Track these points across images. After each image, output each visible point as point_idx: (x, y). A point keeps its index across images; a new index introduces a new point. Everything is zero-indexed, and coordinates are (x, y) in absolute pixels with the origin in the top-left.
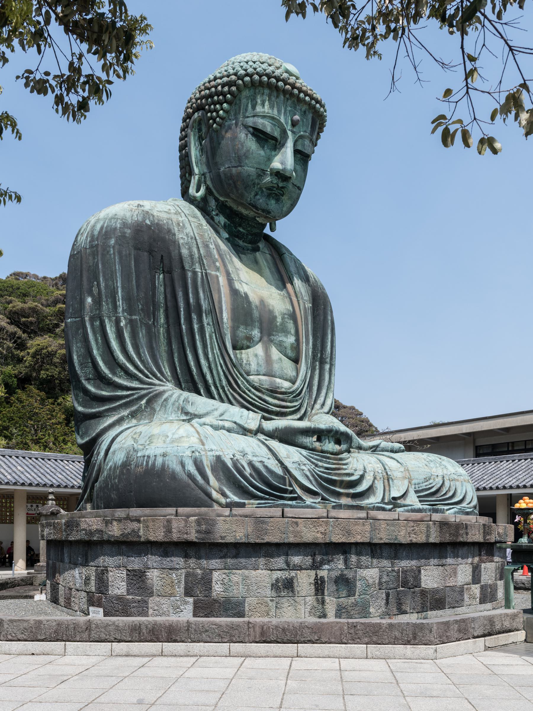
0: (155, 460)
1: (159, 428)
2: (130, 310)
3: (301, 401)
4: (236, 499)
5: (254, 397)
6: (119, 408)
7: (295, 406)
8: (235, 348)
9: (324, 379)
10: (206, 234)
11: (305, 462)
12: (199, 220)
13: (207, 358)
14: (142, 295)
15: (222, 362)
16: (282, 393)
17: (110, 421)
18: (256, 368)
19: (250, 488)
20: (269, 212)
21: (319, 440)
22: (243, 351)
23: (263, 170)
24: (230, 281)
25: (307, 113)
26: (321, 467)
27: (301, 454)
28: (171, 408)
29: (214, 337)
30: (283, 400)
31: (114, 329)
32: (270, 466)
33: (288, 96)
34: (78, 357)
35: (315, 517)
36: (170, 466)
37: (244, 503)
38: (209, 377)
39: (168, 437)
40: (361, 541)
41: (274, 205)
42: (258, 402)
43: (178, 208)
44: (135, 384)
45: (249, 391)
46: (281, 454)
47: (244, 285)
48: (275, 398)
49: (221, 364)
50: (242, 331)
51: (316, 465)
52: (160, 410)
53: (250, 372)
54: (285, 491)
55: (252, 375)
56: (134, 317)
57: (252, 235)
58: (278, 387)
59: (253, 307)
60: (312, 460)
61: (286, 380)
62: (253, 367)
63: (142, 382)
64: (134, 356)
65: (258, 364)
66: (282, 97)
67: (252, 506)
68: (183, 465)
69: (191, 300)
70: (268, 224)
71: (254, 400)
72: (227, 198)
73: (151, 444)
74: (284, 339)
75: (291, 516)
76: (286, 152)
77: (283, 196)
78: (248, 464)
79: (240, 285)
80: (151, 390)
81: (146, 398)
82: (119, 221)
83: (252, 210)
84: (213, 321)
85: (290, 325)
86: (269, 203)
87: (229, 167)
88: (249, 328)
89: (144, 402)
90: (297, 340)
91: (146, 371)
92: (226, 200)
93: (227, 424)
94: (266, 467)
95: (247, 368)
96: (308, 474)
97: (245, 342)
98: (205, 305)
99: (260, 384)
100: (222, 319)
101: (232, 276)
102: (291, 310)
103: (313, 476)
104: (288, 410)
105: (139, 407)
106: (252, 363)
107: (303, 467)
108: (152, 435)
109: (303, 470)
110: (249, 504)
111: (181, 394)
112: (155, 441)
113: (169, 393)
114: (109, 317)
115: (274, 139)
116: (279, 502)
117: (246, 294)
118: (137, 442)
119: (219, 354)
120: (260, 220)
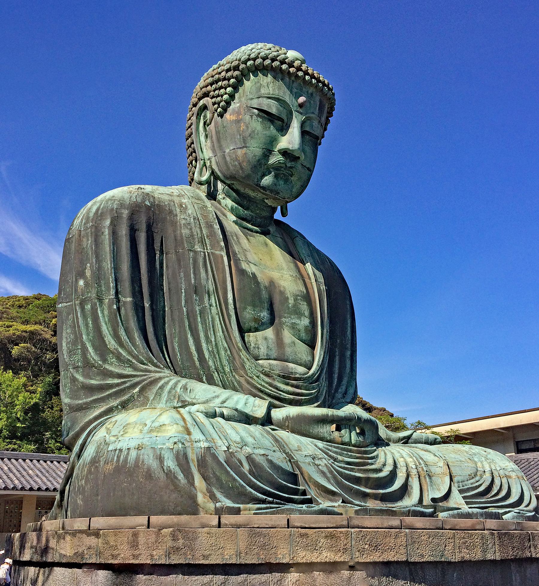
0: (128, 454)
1: (137, 415)
4: (229, 503)
5: (263, 383)
6: (108, 398)
7: (311, 394)
9: (345, 367)
10: (211, 215)
11: (320, 456)
12: (204, 202)
15: (226, 345)
16: (296, 379)
17: (97, 412)
18: (266, 353)
19: (248, 487)
21: (338, 429)
22: (251, 334)
23: (270, 150)
25: (314, 95)
26: (341, 461)
27: (316, 446)
28: (166, 396)
29: (218, 319)
30: (297, 387)
31: (106, 312)
32: (275, 461)
33: (293, 78)
34: (68, 343)
35: (332, 526)
36: (146, 462)
37: (239, 508)
38: (211, 363)
39: (146, 425)
40: (395, 559)
41: (283, 186)
42: (268, 389)
43: (181, 192)
44: (128, 371)
45: (258, 377)
46: (290, 446)
47: (252, 265)
48: (287, 384)
49: (225, 348)
51: (335, 460)
52: (154, 399)
53: (259, 356)
54: (296, 492)
55: (261, 359)
57: (261, 218)
58: (292, 373)
60: (330, 453)
61: (300, 365)
62: (263, 351)
63: (136, 369)
65: (268, 347)
66: (287, 79)
67: (249, 513)
68: (161, 459)
69: (193, 281)
70: (279, 208)
71: (264, 386)
72: (233, 181)
73: (125, 435)
74: (298, 321)
75: (299, 525)
76: (293, 132)
77: (292, 177)
78: (247, 457)
80: (145, 377)
81: (139, 387)
82: (116, 202)
83: (260, 192)
84: (216, 303)
85: (304, 307)
87: (234, 149)
89: (137, 389)
90: (313, 323)
92: (232, 182)
93: (226, 412)
94: (270, 462)
95: (256, 352)
96: (325, 469)
97: (253, 324)
99: (270, 369)
101: (239, 256)
102: (305, 291)
103: (331, 472)
105: (130, 396)
106: (260, 346)
107: (317, 462)
108: (128, 424)
109: (318, 465)
110: (245, 510)
111: (179, 381)
112: (130, 430)
113: (166, 379)
115: (281, 120)
116: (286, 507)
117: (254, 274)
118: (110, 433)
119: (222, 337)
120: (269, 202)
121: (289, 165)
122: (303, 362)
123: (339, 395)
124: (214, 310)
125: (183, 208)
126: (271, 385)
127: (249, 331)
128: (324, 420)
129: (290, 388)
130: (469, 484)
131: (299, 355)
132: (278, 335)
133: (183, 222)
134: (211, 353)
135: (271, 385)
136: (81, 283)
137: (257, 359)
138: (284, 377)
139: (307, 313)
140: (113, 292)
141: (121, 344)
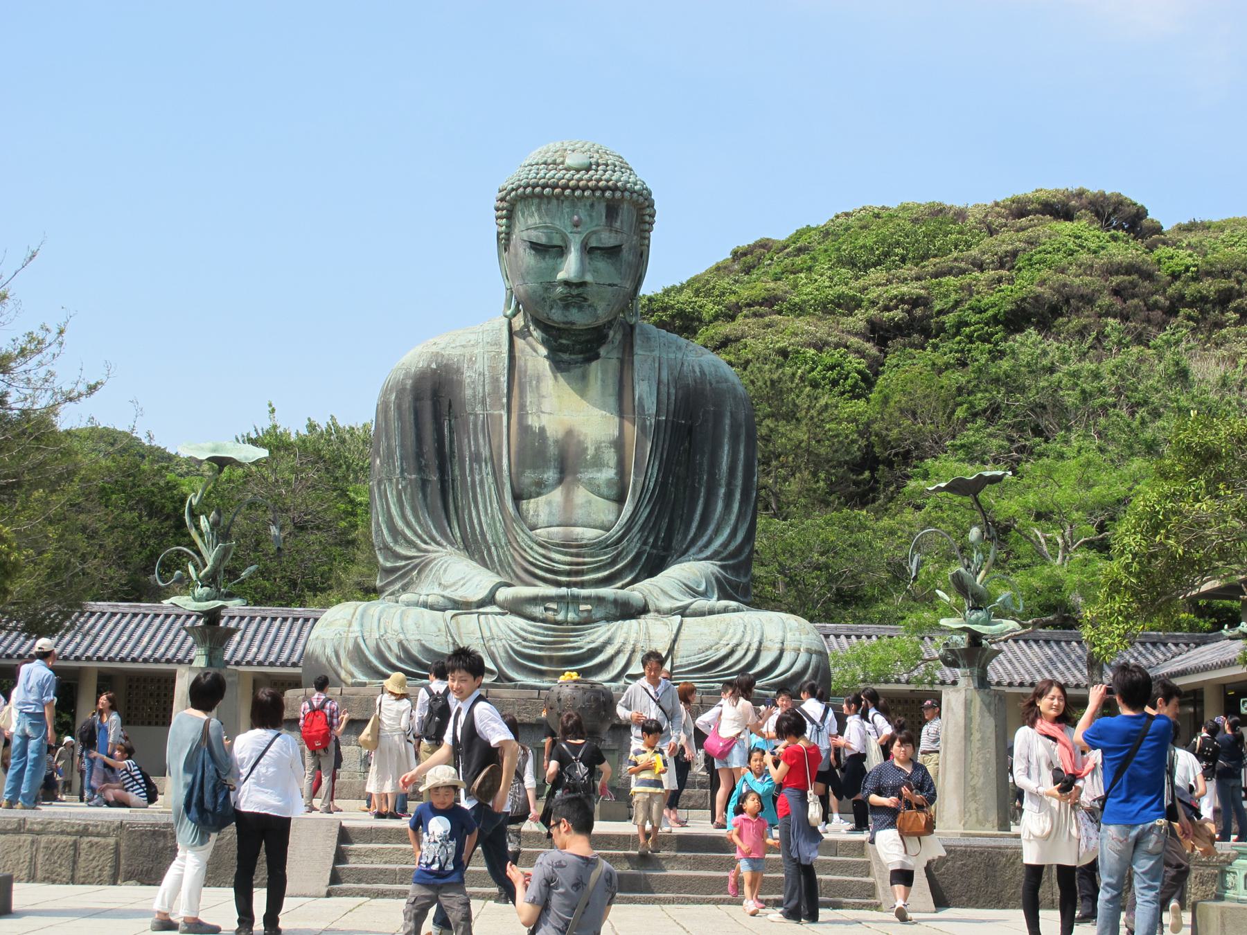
8: (518, 498)
13: (486, 513)
20: (573, 324)
24: (522, 417)
30: (577, 555)
38: (489, 537)
48: (566, 554)
50: (529, 477)
51: (525, 640)
56: (414, 476)
58: (576, 540)
59: (550, 442)
62: (543, 518)
65: (550, 513)
79: (535, 418)
85: (610, 457)
98: (485, 452)
100: (501, 466)
103: (507, 652)
106: (541, 513)
114: (390, 480)
117: (542, 430)
121: (575, 292)
123: (693, 550)
124: (491, 479)
125: (472, 361)
126: (544, 557)
127: (530, 497)
128: (535, 600)
129: (568, 559)
130: (694, 659)
131: (594, 516)
132: (568, 499)
133: (468, 380)
134: (488, 525)
135: (544, 557)
136: (378, 461)
137: (533, 528)
138: (564, 546)
140: (398, 471)
141: (408, 525)
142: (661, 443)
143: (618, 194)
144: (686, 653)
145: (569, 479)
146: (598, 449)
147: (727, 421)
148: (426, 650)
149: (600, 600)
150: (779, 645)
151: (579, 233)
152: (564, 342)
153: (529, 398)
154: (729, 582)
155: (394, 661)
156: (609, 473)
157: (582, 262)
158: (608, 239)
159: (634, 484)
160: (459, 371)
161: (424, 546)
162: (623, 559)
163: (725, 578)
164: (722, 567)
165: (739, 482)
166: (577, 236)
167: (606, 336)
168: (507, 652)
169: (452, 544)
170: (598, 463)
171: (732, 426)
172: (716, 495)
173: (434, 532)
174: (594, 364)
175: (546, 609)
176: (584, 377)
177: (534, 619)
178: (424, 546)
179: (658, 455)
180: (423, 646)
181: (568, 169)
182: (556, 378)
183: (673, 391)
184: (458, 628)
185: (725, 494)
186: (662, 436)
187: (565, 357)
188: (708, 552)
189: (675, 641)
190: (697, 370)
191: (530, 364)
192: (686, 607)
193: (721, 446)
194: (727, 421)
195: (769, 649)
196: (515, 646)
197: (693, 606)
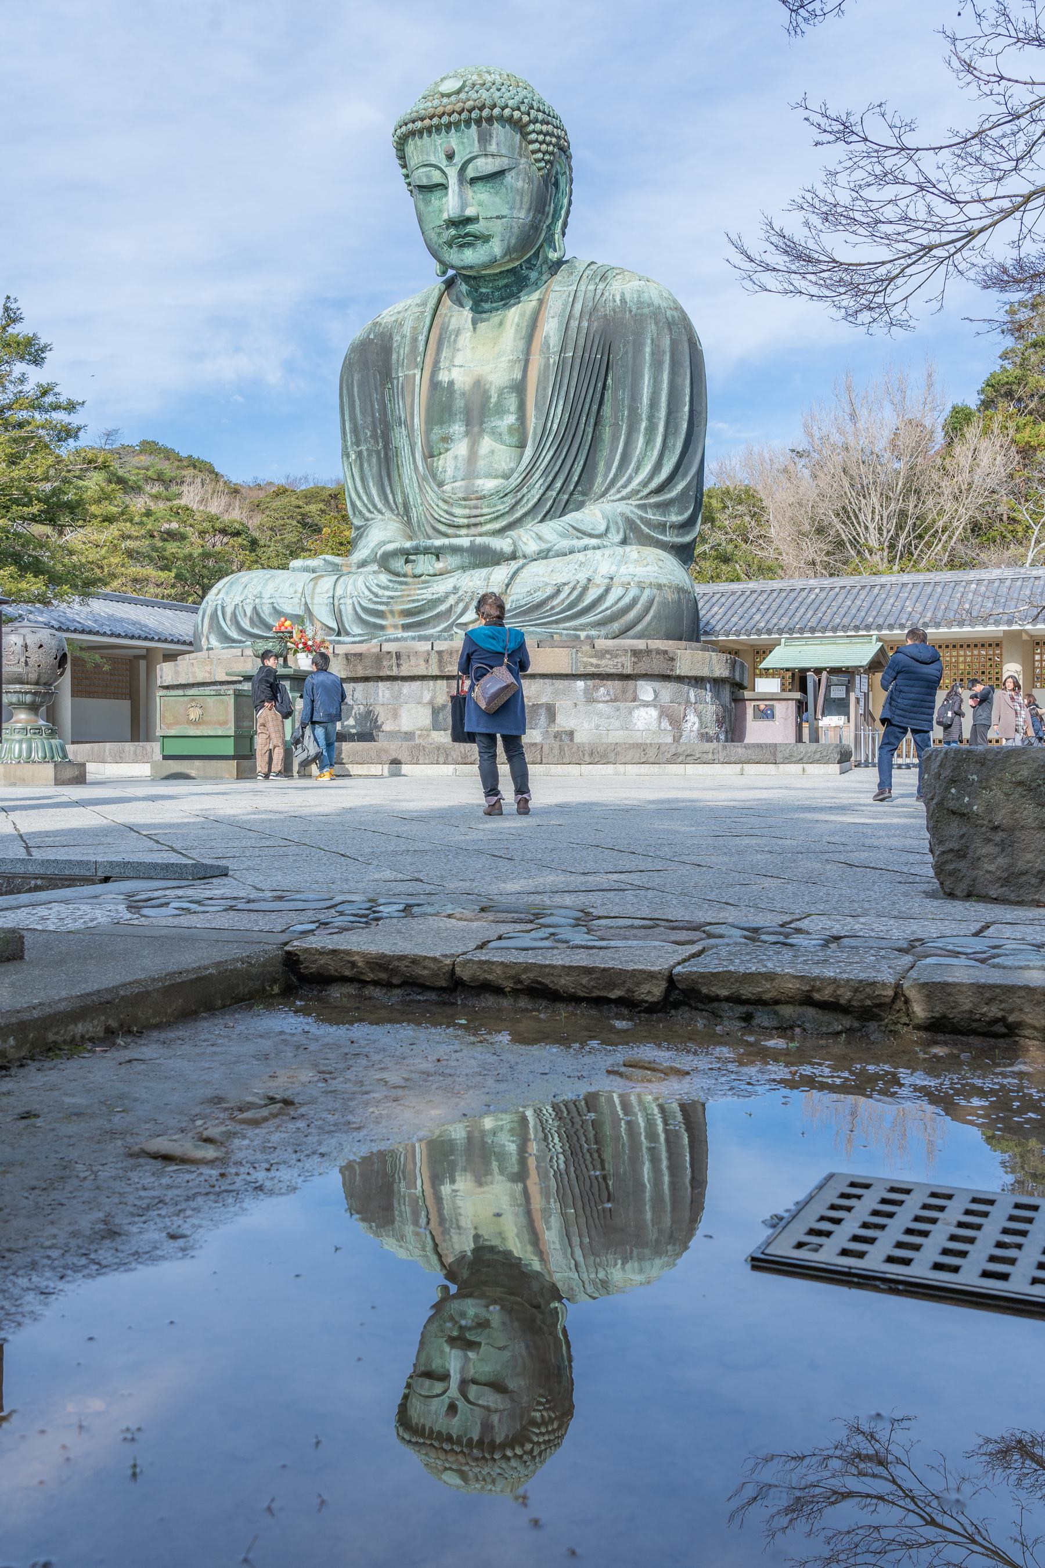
2: (358, 443)
3: (513, 501)
14: (369, 419)
22: (442, 456)
30: (476, 508)
48: (465, 507)
50: (437, 432)
51: (377, 596)
61: (496, 477)
62: (450, 472)
64: (361, 491)
79: (446, 373)
85: (512, 402)
86: (463, 257)
88: (444, 426)
91: (370, 506)
95: (442, 477)
100: (413, 425)
103: (354, 609)
104: (482, 519)
106: (448, 469)
117: (451, 383)
122: (499, 473)
123: (612, 491)
127: (440, 454)
129: (467, 512)
135: (447, 512)
137: (440, 485)
138: (465, 499)
139: (513, 408)
141: (360, 497)
142: (566, 381)
143: (485, 113)
144: (514, 597)
145: (476, 429)
146: (500, 394)
147: (648, 349)
148: (277, 612)
149: (455, 550)
150: (607, 581)
151: (455, 165)
152: (484, 290)
153: (445, 353)
154: (648, 523)
155: (246, 624)
156: (511, 419)
157: (461, 195)
158: (485, 165)
159: (535, 428)
160: (391, 338)
161: (368, 515)
162: (523, 506)
163: (641, 518)
164: (639, 506)
165: (662, 413)
166: (453, 168)
167: (526, 278)
168: (354, 609)
169: (392, 510)
170: (500, 411)
171: (653, 354)
172: (638, 431)
173: (376, 499)
174: (514, 309)
175: (407, 561)
176: (501, 324)
177: (398, 575)
178: (368, 515)
179: (563, 394)
180: (274, 608)
181: (443, 95)
182: (475, 329)
183: (585, 324)
184: (314, 589)
185: (646, 429)
186: (567, 374)
187: (486, 306)
188: (625, 492)
189: (508, 585)
190: (618, 298)
191: (453, 320)
192: (549, 550)
193: (642, 376)
194: (648, 349)
195: (598, 586)
196: (365, 603)
197: (556, 548)
